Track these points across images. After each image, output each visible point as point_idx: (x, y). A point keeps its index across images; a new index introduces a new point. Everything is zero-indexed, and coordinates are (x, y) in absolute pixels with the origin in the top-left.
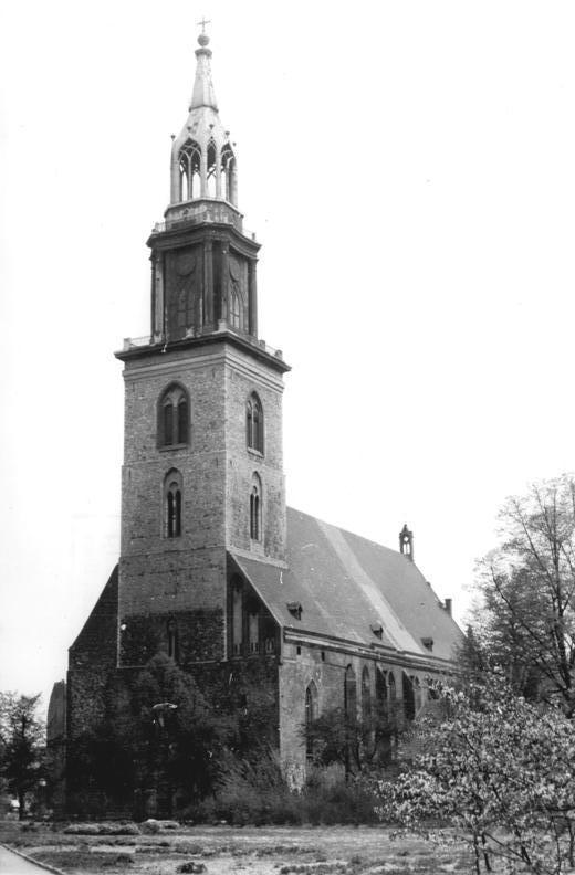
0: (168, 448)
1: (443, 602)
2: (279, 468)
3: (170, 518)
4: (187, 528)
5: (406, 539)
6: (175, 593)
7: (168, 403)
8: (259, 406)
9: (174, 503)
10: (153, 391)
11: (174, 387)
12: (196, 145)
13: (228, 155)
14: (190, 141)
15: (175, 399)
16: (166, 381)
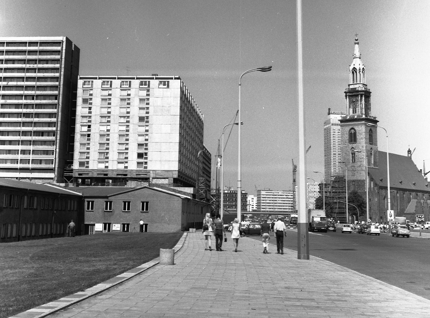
0: (351, 142)
1: (420, 170)
2: (377, 145)
3: (352, 159)
4: (357, 161)
5: (409, 153)
6: (354, 176)
7: (351, 132)
8: (372, 132)
9: (353, 155)
10: (347, 129)
11: (352, 128)
12: (356, 69)
13: (363, 70)
14: (354, 68)
15: (353, 131)
16: (351, 127)
